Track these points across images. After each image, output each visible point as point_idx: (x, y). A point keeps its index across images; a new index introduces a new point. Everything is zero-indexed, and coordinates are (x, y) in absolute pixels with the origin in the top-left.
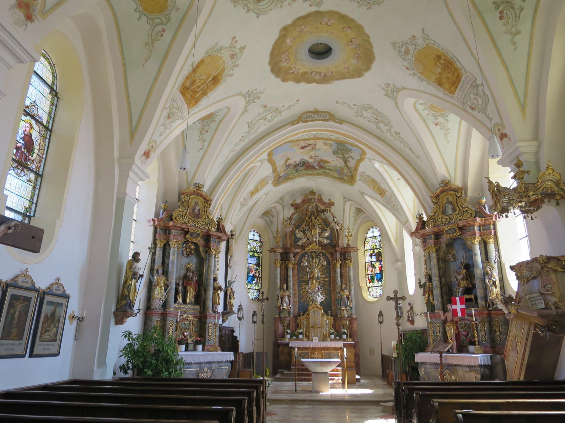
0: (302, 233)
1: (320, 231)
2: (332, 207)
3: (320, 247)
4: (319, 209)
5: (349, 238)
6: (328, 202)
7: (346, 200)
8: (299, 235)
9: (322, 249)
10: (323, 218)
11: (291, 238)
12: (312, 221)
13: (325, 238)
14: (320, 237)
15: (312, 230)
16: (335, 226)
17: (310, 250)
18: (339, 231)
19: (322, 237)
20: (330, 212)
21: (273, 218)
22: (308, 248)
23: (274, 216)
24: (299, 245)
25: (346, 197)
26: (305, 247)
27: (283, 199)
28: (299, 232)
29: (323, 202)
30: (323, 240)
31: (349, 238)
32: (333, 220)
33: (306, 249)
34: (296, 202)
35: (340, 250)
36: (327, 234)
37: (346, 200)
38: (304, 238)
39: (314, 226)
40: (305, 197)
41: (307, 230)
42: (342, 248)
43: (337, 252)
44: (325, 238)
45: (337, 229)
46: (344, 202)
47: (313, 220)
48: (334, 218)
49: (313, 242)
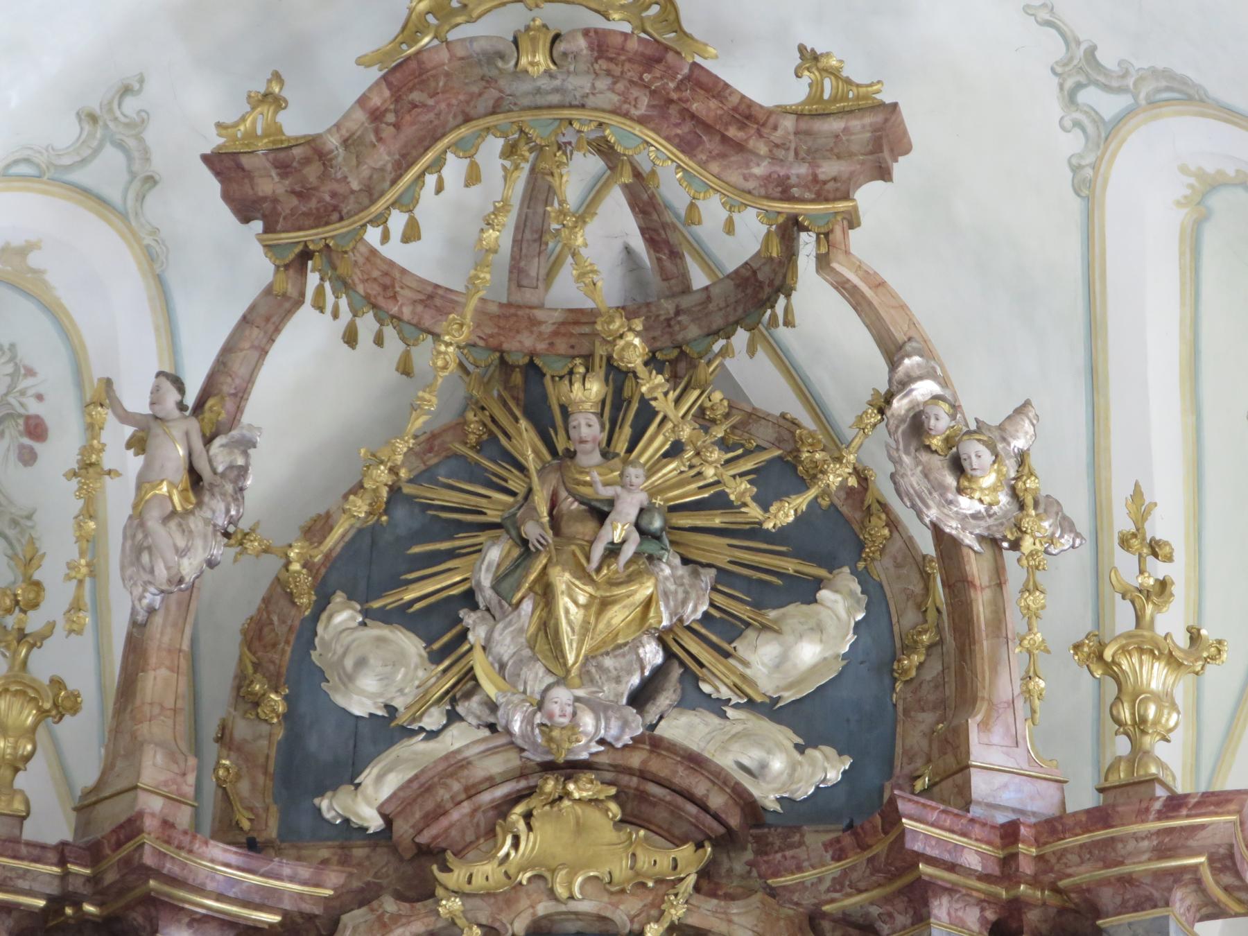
0: (410, 645)
1: (695, 610)
2: (869, 196)
3: (686, 852)
4: (699, 279)
5: (1156, 676)
6: (796, 92)
7: (1109, 105)
8: (368, 682)
9: (708, 881)
10: (754, 416)
11: (242, 729)
12: (561, 458)
13: (771, 709)
14: (693, 698)
15: (562, 579)
16: (914, 480)
17: (509, 894)
18: (977, 567)
19: (717, 707)
20: (823, 262)
21: (28, 458)
22: (485, 873)
23: (36, 429)
24: (349, 830)
25: (1107, 58)
26: (432, 854)
27: (138, 125)
28: (378, 630)
29: (715, 88)
30: (751, 757)
31: (1156, 676)
32: (883, 404)
33: (455, 878)
34: (294, 124)
35: (972, 860)
36: (808, 653)
37: (1109, 105)
38: (433, 720)
39: (600, 513)
40: (411, 29)
41: (486, 595)
42: (1010, 833)
43: (941, 909)
44: (771, 709)
45: (946, 544)
46: (1073, 143)
47: (588, 428)
48: (893, 352)
49: (573, 769)
